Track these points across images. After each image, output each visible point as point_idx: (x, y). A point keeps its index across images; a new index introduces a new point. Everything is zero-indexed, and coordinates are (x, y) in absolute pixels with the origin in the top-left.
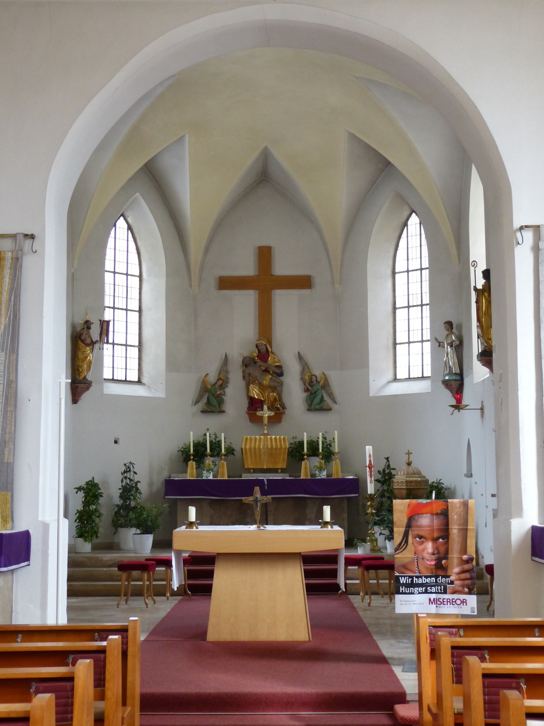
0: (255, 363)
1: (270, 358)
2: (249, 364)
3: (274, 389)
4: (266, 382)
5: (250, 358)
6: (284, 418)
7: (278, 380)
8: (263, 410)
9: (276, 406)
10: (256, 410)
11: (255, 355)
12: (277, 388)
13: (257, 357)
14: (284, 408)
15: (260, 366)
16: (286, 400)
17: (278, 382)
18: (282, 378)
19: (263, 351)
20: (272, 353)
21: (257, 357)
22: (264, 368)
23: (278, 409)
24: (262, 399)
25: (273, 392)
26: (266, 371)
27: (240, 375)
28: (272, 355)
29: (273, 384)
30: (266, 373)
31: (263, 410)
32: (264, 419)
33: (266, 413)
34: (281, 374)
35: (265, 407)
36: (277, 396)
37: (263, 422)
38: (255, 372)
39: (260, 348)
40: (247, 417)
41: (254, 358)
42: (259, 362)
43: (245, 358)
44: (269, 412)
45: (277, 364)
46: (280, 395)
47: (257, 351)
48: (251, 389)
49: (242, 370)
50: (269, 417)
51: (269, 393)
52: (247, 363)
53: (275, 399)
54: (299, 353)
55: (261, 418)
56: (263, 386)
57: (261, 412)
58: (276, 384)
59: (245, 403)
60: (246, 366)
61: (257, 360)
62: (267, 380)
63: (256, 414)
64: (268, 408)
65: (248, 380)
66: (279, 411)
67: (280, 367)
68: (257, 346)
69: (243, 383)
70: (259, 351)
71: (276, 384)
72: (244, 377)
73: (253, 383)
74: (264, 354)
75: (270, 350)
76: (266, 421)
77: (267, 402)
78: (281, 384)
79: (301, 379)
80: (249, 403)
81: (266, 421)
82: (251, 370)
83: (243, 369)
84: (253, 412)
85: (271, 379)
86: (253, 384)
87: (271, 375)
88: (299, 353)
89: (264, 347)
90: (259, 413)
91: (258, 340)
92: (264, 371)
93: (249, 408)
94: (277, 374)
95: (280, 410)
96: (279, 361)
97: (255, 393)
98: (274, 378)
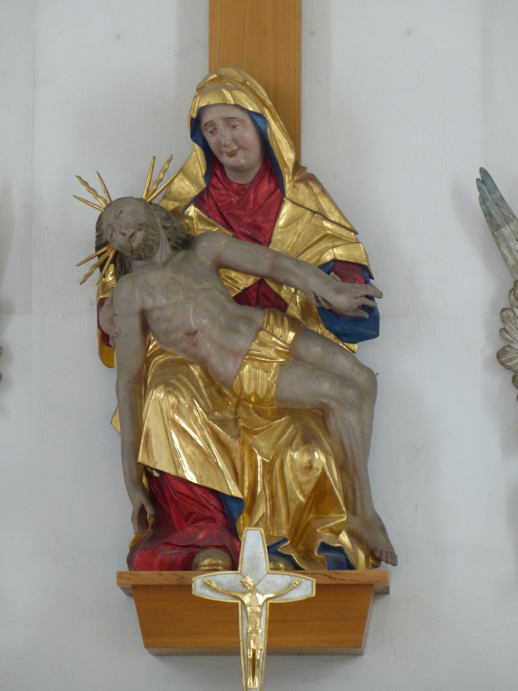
0: (185, 243)
1: (286, 210)
2: (145, 253)
3: (311, 422)
4: (255, 378)
5: (149, 205)
6: (383, 618)
7: (341, 362)
8: (234, 566)
9: (327, 537)
10: (188, 564)
11: (186, 188)
12: (332, 418)
13: (198, 201)
14: (380, 554)
15: (220, 265)
16: (391, 500)
17: (342, 379)
18: (365, 351)
19: (241, 160)
20: (306, 178)
21: (198, 201)
22: (245, 282)
23: (342, 561)
24: (234, 491)
25: (308, 440)
26: (262, 297)
27: (83, 328)
28: (302, 193)
29: (308, 388)
30: (258, 315)
31: (234, 566)
32: (244, 627)
33: (256, 583)
34: (360, 324)
35: (253, 543)
36: (334, 476)
37: (234, 651)
38: (183, 301)
39: (220, 138)
40: (124, 611)
41: (179, 213)
42: (215, 241)
43: (114, 207)
44: (282, 579)
45: (339, 253)
46: (352, 467)
47: (198, 166)
48: (152, 421)
49: (90, 292)
50: (280, 614)
51: (279, 453)
52: (128, 243)
53: (320, 493)
54: (485, 180)
55: (228, 614)
56: (241, 400)
57: (225, 578)
58: (326, 387)
59: (112, 520)
60: (122, 263)
61: (200, 228)
62: (263, 359)
63: (189, 587)
64: (274, 551)
65: (138, 357)
66: (345, 576)
67: (354, 272)
68: (197, 128)
69: (97, 386)
70: (212, 160)
71: (326, 387)
72: (105, 338)
73: (171, 377)
74: (244, 187)
75: (286, 154)
76: (255, 637)
77: (262, 509)
78: (365, 390)
79: (501, 356)
80: (141, 516)
81: (255, 637)
82: (155, 288)
83: (104, 287)
84: (169, 577)
85: (292, 354)
86: (170, 388)
87: (294, 324)
88: (485, 180)
89: (250, 135)
90: (209, 584)
91: (201, 90)
92: (243, 298)
93: (140, 556)
94: (329, 315)
95: (350, 566)
96: (350, 232)
97: (183, 445)
98: (314, 350)
